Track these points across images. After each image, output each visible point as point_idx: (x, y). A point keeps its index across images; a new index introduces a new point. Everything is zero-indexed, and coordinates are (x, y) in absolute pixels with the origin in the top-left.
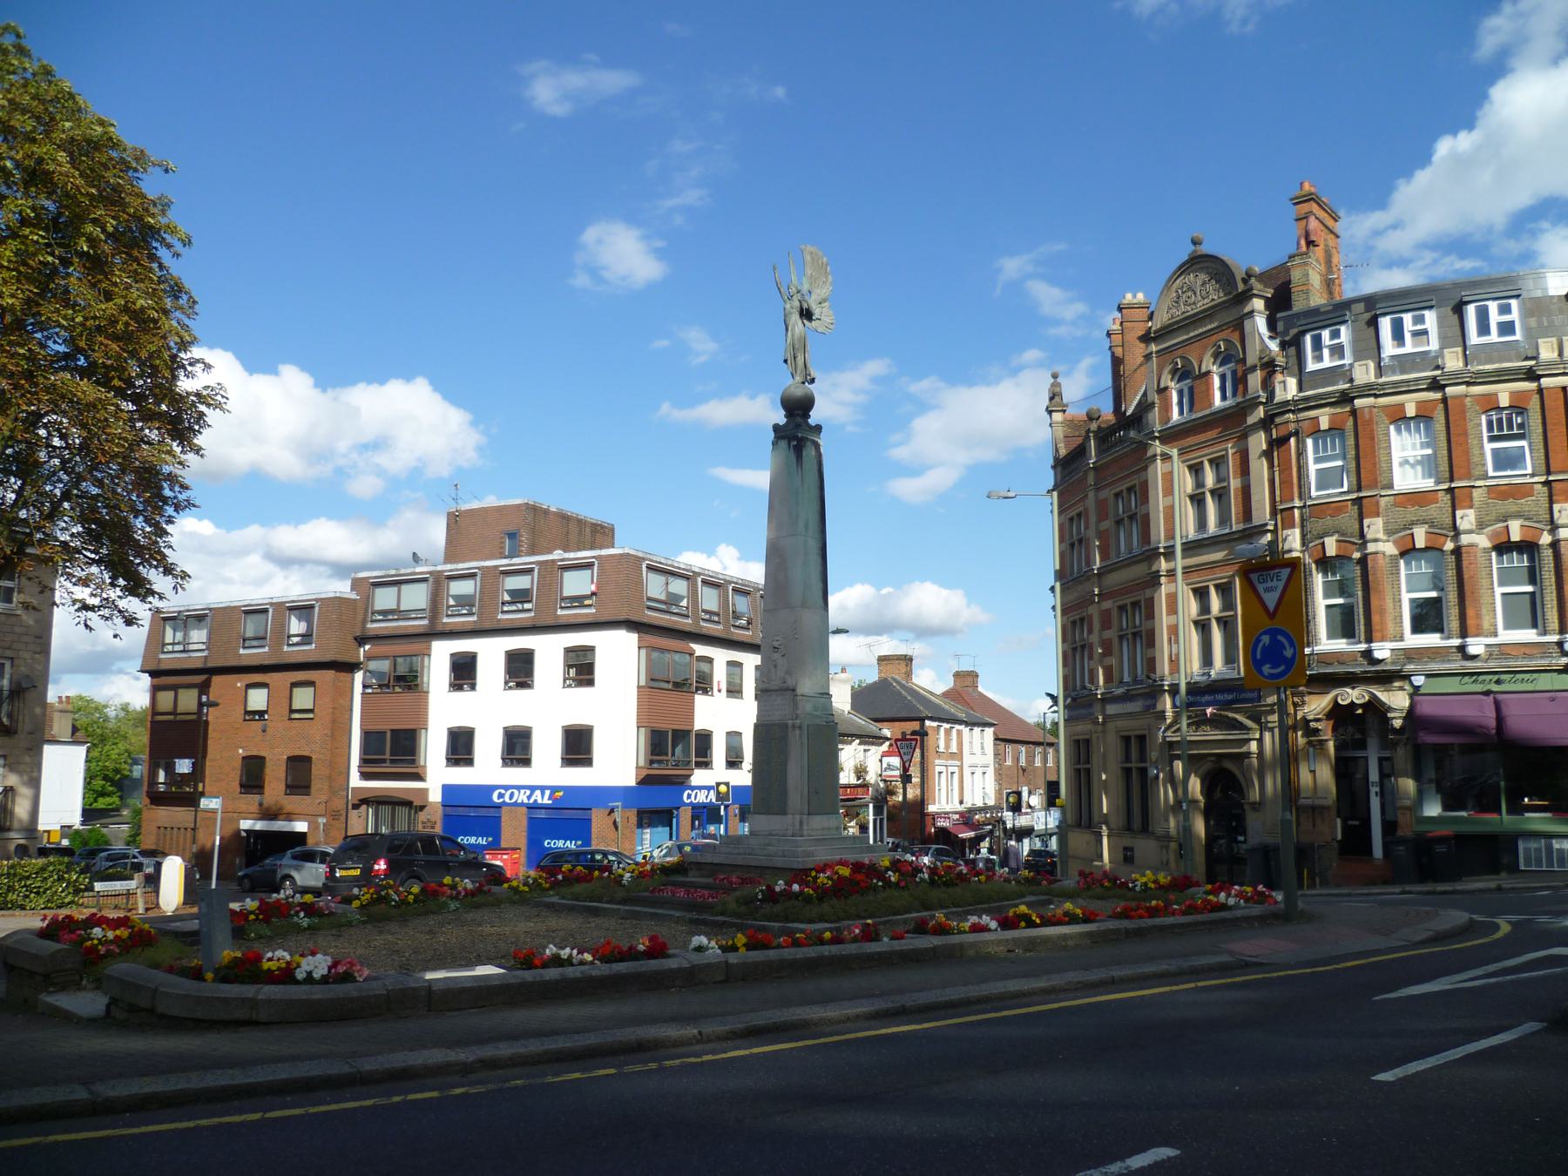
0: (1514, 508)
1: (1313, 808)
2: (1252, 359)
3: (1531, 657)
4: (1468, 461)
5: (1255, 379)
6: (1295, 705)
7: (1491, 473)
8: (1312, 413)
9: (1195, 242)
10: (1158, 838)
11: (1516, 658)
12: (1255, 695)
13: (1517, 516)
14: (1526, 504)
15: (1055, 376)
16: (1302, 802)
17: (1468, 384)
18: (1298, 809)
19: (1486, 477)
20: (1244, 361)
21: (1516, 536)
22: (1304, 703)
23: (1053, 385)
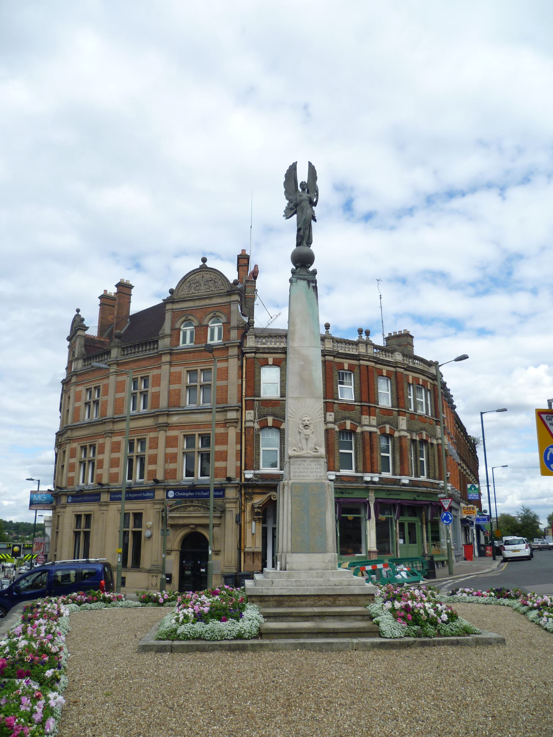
0: (348, 415)
1: (253, 553)
2: (234, 323)
3: (352, 482)
4: (333, 390)
5: (234, 334)
6: (246, 499)
7: (340, 398)
8: (265, 356)
9: (204, 260)
10: (149, 571)
11: (346, 482)
12: (221, 493)
13: (349, 418)
14: (352, 414)
15: (78, 311)
16: (246, 550)
17: (334, 356)
18: (244, 553)
19: (338, 399)
20: (229, 323)
21: (348, 427)
22: (252, 499)
23: (76, 315)
